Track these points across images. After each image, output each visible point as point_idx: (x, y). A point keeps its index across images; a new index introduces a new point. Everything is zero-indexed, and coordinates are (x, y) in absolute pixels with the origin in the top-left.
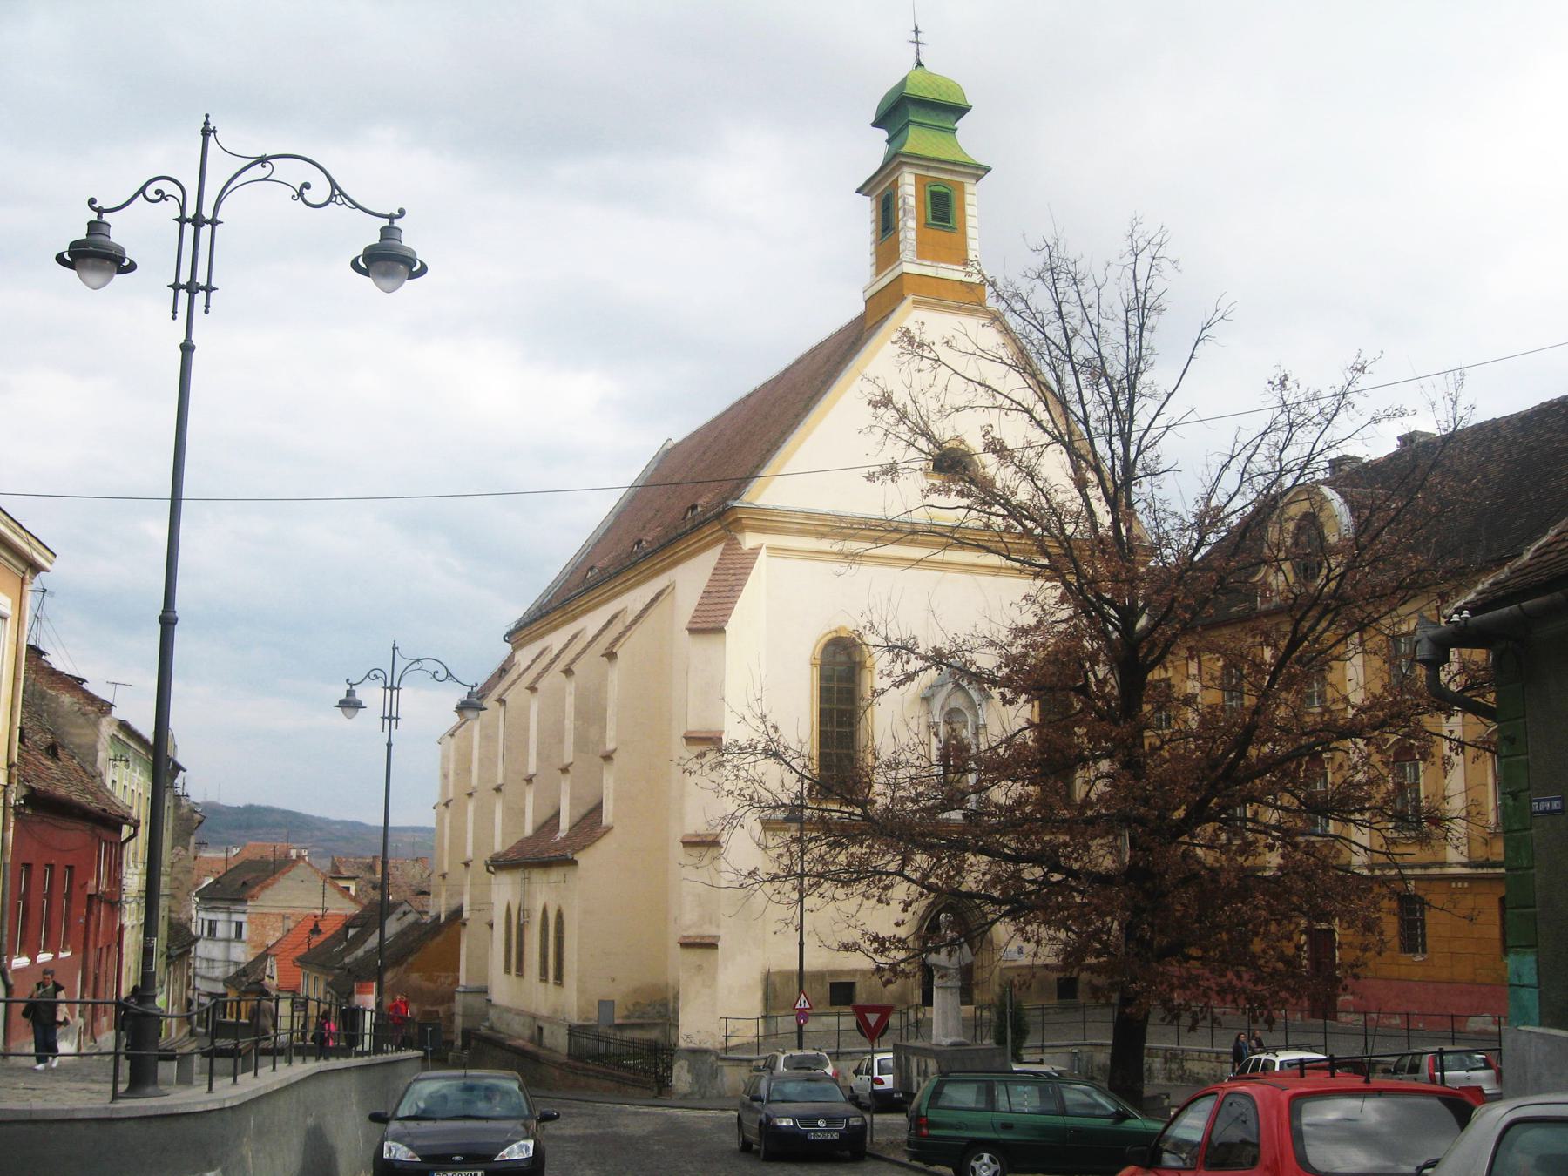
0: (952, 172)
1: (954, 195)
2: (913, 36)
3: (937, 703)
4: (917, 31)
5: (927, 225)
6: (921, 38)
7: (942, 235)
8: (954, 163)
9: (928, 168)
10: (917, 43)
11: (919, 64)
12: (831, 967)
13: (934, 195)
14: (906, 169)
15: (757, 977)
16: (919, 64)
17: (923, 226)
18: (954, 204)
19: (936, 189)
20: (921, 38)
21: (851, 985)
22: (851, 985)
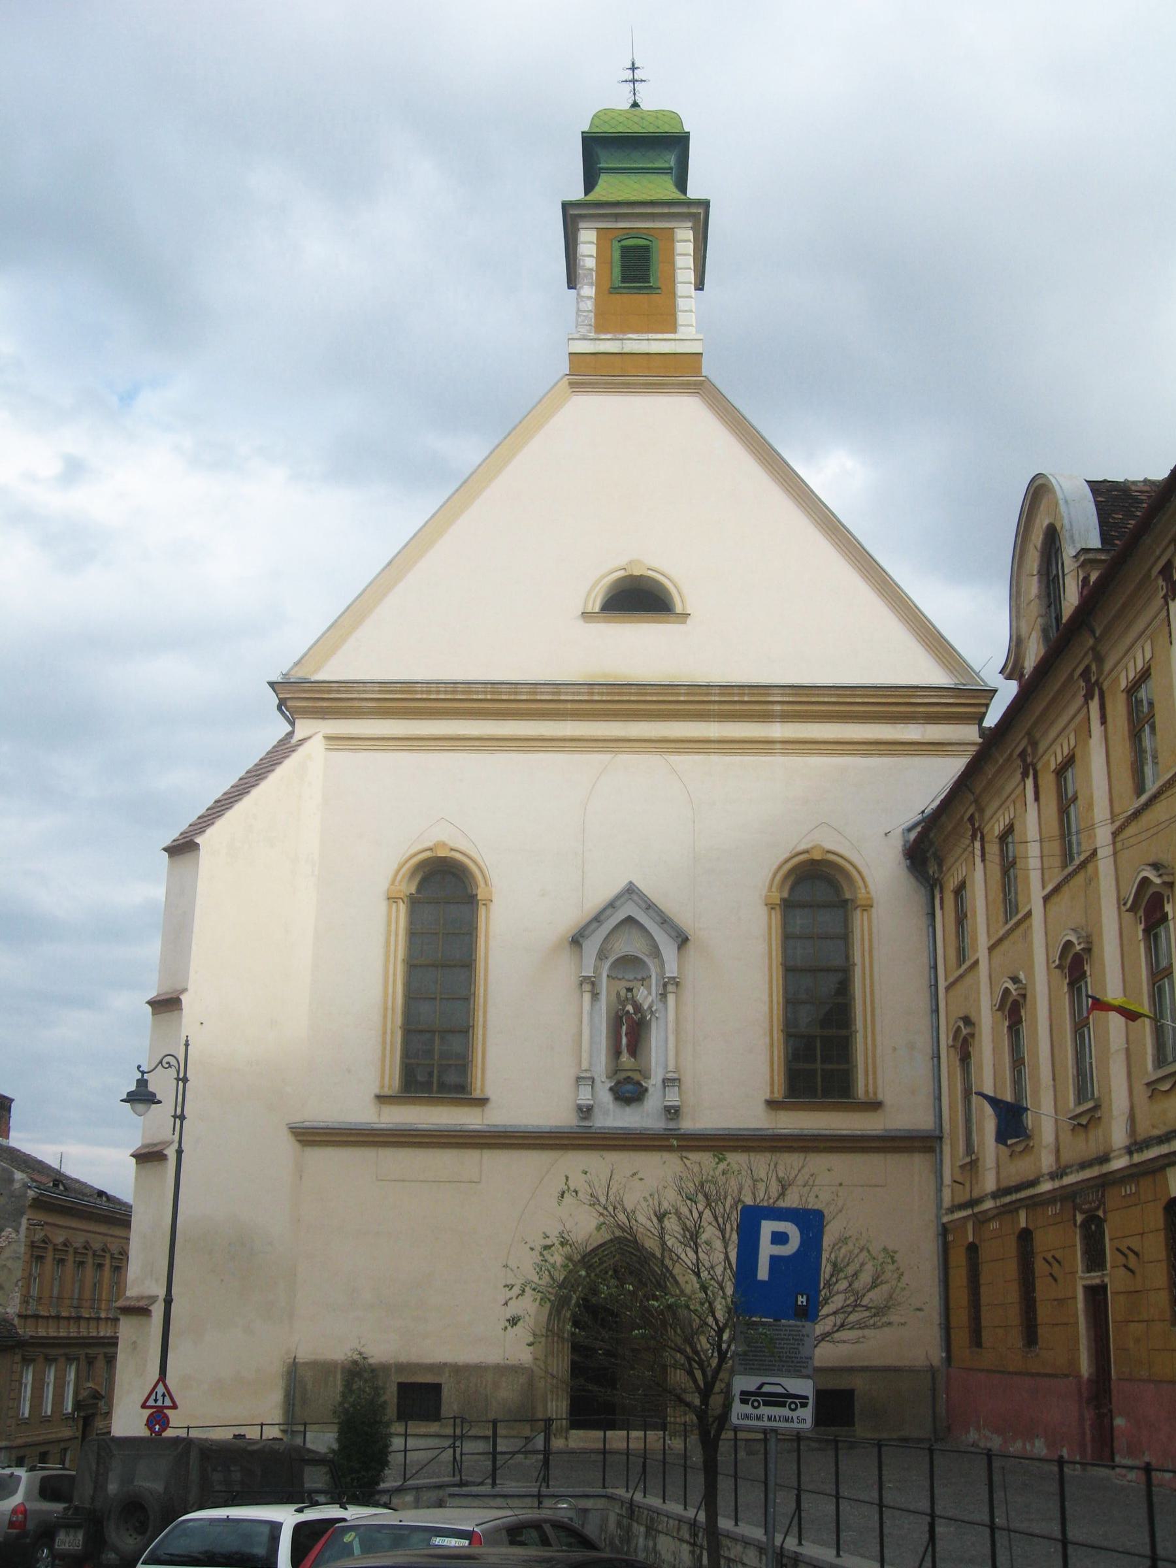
0: (653, 217)
1: (657, 247)
2: (628, 75)
3: (592, 946)
4: (633, 68)
5: (614, 290)
6: (639, 75)
7: (639, 301)
8: (652, 203)
9: (617, 217)
10: (634, 81)
11: (635, 105)
12: (403, 1359)
13: (626, 252)
14: (581, 225)
15: (276, 1368)
16: (635, 105)
17: (608, 291)
18: (656, 257)
19: (625, 243)
20: (639, 75)
21: (436, 1388)
22: (436, 1388)
